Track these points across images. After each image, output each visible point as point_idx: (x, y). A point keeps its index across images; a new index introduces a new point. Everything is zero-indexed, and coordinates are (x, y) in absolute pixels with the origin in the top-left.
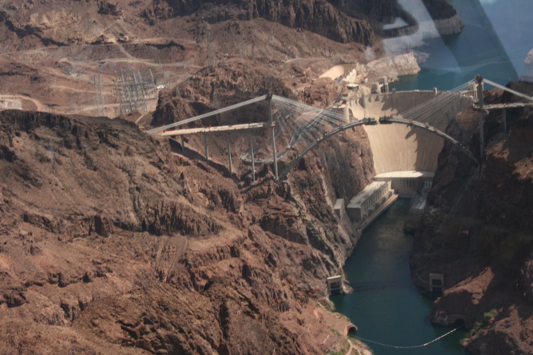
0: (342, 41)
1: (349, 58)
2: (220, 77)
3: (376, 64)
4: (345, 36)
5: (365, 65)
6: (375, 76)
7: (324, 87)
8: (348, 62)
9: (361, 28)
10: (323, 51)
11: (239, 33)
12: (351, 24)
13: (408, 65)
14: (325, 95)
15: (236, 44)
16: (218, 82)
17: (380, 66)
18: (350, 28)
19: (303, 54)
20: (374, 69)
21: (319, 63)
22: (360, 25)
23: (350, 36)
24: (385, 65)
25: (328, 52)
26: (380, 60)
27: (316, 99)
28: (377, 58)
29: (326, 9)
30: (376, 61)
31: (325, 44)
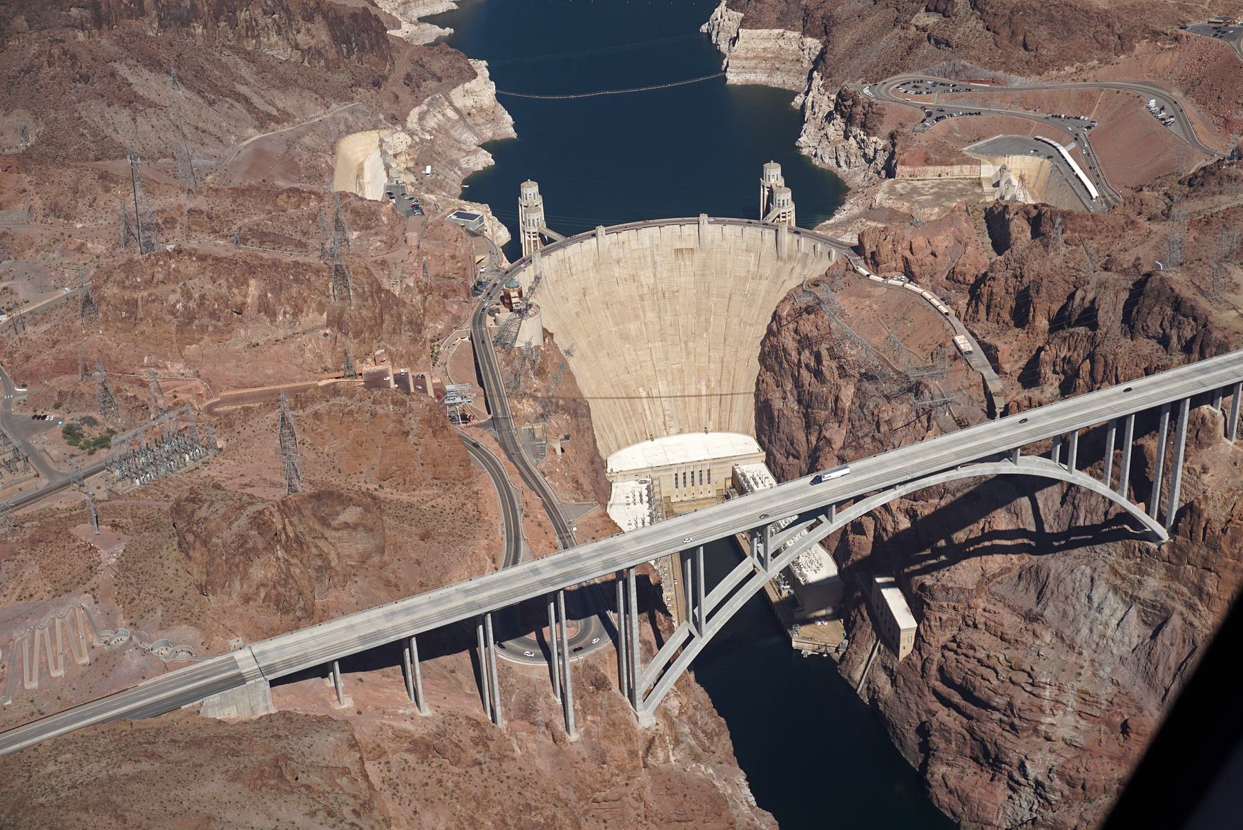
2: (190, 283)
3: (422, 117)
5: (404, 129)
7: (453, 257)
11: (85, 79)
13: (481, 109)
14: (461, 279)
15: (84, 113)
16: (192, 304)
17: (431, 123)
19: (264, 120)
20: (428, 137)
21: (307, 140)
24: (440, 116)
26: (424, 107)
27: (445, 296)
28: (418, 102)
31: (296, 81)
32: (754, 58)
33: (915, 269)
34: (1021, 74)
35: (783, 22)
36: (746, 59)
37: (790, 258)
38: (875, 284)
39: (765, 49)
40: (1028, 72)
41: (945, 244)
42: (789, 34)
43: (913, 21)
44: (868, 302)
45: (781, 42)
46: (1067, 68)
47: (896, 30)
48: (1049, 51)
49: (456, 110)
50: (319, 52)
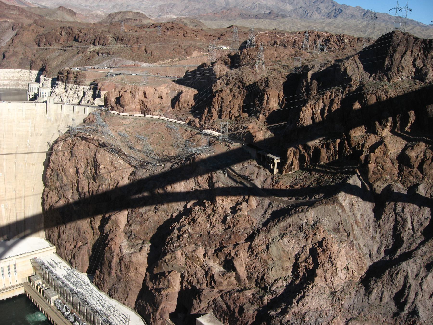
32: (8, 80)
33: (149, 106)
34: (148, 62)
35: (21, 66)
36: (4, 80)
37: (56, 120)
38: (124, 118)
39: (13, 77)
40: (150, 61)
41: (166, 91)
42: (23, 70)
43: (88, 50)
44: (122, 128)
45: (21, 74)
46: (166, 60)
47: (80, 55)
48: (157, 53)
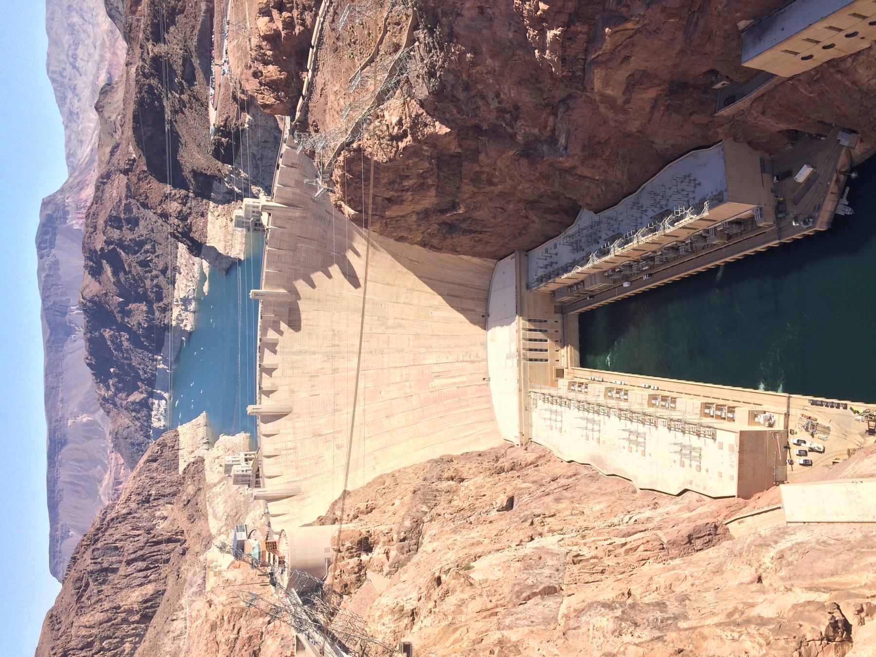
0: (159, 594)
1: (194, 574)
3: (215, 517)
4: (149, 589)
6: (237, 513)
8: (202, 575)
9: (140, 553)
10: (171, 635)
12: (126, 576)
18: (136, 578)
20: (224, 519)
22: (133, 556)
23: (152, 577)
24: (220, 498)
25: (175, 623)
26: (210, 511)
28: (206, 517)
29: (84, 632)
30: (210, 518)
49: (220, 482)
50: (146, 601)
